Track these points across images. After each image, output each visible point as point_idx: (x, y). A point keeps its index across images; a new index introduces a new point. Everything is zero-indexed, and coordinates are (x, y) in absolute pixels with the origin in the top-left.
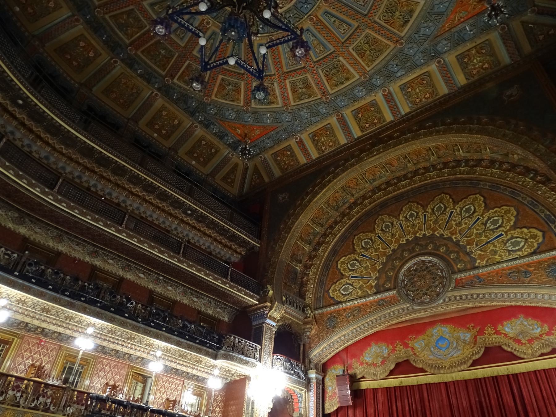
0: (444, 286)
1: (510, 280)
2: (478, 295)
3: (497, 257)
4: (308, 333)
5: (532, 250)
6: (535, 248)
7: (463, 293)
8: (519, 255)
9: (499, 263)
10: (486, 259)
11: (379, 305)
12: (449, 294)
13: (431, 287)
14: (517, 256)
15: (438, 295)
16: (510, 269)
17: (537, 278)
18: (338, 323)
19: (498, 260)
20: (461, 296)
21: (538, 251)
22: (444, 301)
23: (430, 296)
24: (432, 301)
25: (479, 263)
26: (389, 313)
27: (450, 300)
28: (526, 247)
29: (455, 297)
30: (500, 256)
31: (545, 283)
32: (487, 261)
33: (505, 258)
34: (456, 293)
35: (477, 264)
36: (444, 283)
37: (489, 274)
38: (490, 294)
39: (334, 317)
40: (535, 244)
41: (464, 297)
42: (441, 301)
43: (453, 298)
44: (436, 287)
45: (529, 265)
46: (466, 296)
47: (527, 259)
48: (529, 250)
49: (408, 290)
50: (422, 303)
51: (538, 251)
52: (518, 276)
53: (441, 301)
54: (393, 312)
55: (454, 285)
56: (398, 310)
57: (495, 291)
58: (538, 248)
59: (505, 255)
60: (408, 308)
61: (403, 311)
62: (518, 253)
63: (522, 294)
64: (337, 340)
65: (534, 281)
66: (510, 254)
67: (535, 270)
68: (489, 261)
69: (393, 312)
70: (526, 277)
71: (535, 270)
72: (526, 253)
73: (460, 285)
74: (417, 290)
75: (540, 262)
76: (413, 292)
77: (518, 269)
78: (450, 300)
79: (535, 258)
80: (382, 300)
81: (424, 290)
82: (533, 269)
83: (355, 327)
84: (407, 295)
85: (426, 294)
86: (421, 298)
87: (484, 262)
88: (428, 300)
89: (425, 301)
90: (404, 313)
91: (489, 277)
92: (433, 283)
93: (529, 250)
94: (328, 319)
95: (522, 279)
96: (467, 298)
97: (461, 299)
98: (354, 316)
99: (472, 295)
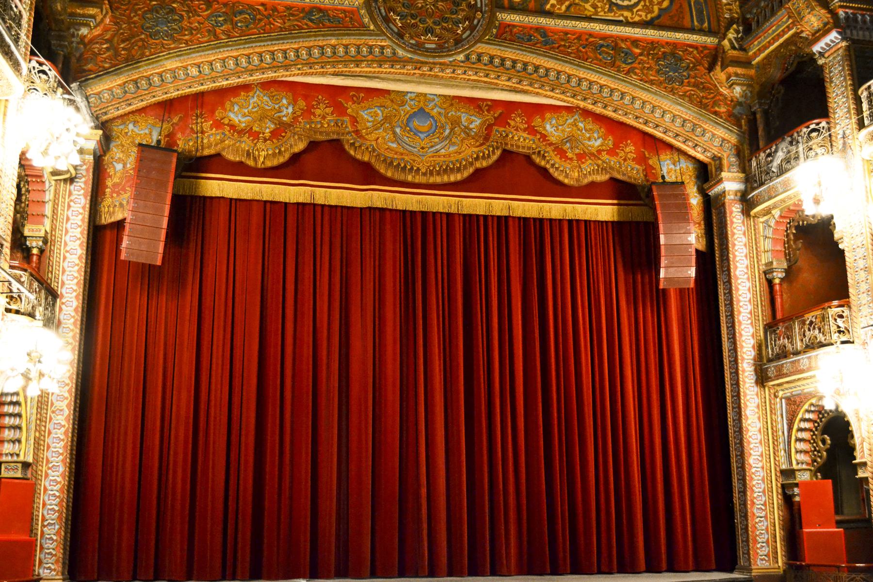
0: (472, 28)
1: (597, 59)
2: (537, 68)
3: (588, 6)
4: (84, 31)
5: (649, 16)
6: (653, 15)
7: (510, 54)
8: (626, 18)
9: (589, 19)
10: (567, 3)
11: (312, 21)
12: (481, 48)
13: (446, 20)
14: (621, 18)
15: (458, 41)
16: (604, 37)
17: (642, 69)
18: (182, 28)
19: (589, 14)
20: (503, 60)
21: (656, 22)
22: (467, 58)
23: (440, 37)
24: (441, 49)
25: (553, 6)
26: (334, 47)
27: (479, 60)
28: (640, 7)
29: (492, 58)
30: (595, 6)
31: (652, 82)
32: (568, 8)
33: (602, 15)
34: (494, 50)
35: (548, 7)
36: (475, 22)
37: (566, 33)
38: (559, 73)
39: (173, 11)
40: (656, 8)
41: (508, 63)
42: (461, 57)
43: (486, 59)
44: (457, 23)
45: (635, 42)
46: (514, 62)
47: (637, 30)
48: (643, 14)
49: (391, 9)
50: (419, 48)
51: (656, 22)
52: (614, 55)
53: (461, 57)
54: (346, 47)
55: (495, 31)
56: (358, 47)
57: (568, 69)
58: (659, 17)
59: (603, 10)
60: (382, 48)
61: (371, 53)
62: (626, 13)
63: (612, 91)
64: (173, 71)
65: (636, 74)
66: (610, 10)
67: (641, 54)
68: (572, 9)
69: (346, 47)
70: (624, 62)
71: (641, 54)
72: (637, 19)
73: (507, 35)
74: (413, 16)
75: (653, 44)
76: (403, 17)
77: (616, 44)
78: (479, 60)
79: (651, 34)
80: (320, 10)
81: (430, 22)
82: (638, 51)
83: (235, 54)
84: (387, 20)
85: (429, 30)
86: (418, 36)
87: (564, 8)
88: (433, 46)
89: (427, 46)
90: (370, 57)
91: (563, 40)
92: (452, 13)
93: (643, 14)
94: (151, 11)
95: (618, 63)
96: (514, 67)
97: (502, 64)
98: (235, 25)
99: (525, 64)
